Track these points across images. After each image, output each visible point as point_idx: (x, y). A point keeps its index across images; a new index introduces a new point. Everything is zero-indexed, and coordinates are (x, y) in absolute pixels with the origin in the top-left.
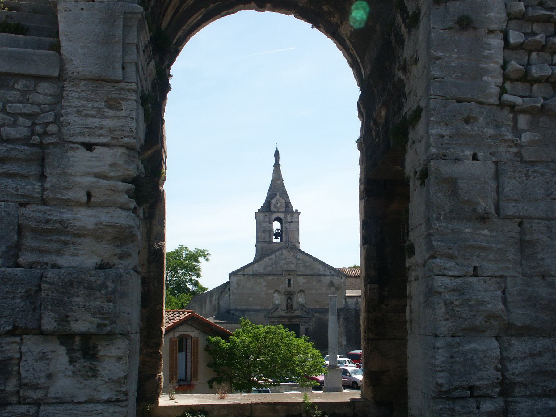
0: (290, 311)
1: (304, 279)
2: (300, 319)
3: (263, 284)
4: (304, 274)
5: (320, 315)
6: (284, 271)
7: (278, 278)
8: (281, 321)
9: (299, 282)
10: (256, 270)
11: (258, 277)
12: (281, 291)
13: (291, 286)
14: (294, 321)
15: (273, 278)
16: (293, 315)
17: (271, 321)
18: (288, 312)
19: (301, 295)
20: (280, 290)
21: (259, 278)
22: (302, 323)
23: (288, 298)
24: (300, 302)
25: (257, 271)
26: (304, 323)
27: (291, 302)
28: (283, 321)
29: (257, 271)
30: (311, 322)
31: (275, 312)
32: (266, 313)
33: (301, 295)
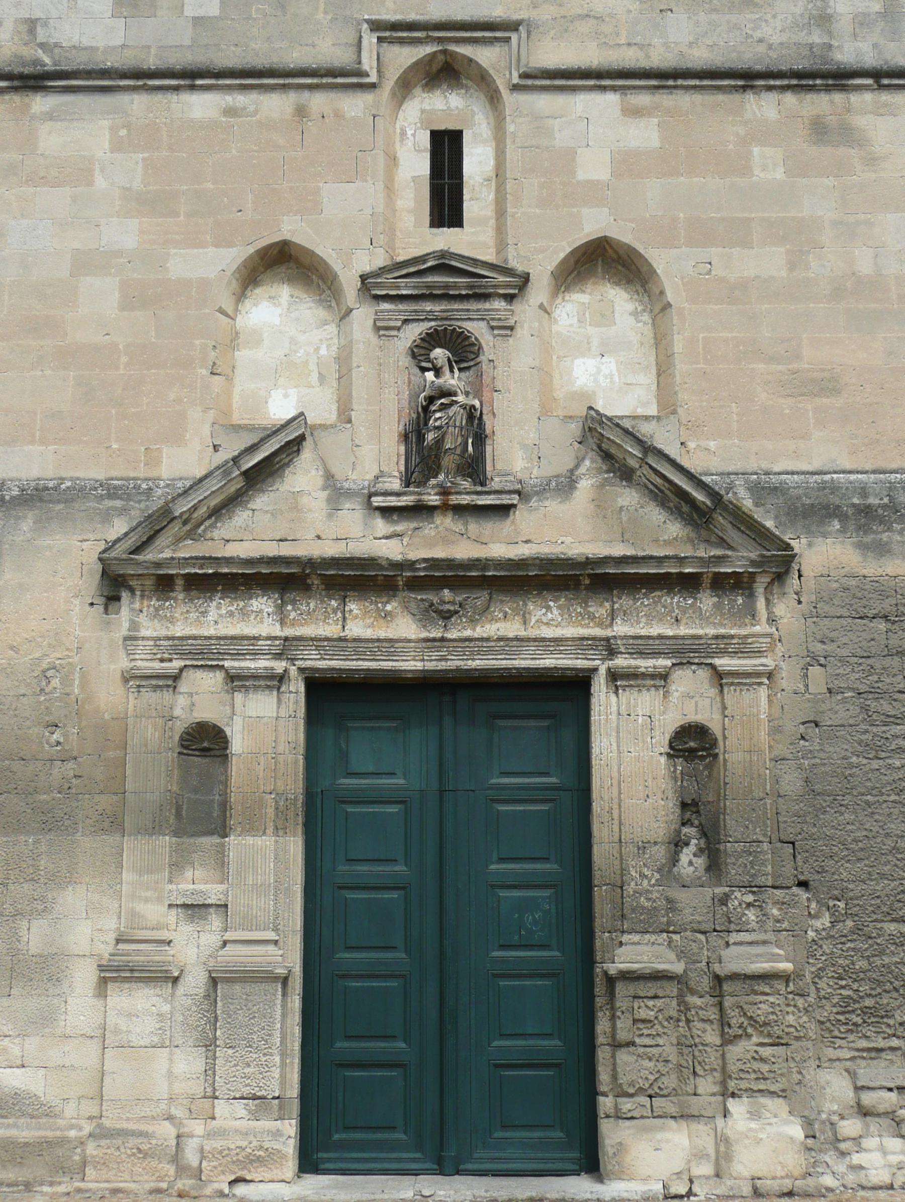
0: (445, 492)
1: (635, 113)
2: (601, 610)
3: (100, 182)
4: (630, 58)
5: (881, 550)
6: (376, 26)
7: (301, 112)
8: (330, 630)
9: (569, 156)
10: (32, 25)
11: (40, 103)
12: (336, 265)
13: (470, 208)
14: (511, 628)
15: (230, 112)
16: (499, 550)
17: (179, 630)
18: (420, 510)
19: (605, 317)
20: (325, 250)
21: (50, 116)
22: (621, 662)
23: (432, 340)
24: (582, 395)
25: (41, 35)
26: (645, 664)
27: (478, 394)
28: (357, 629)
29: (41, 35)
30: (743, 649)
31: (240, 517)
32: (119, 527)
33: (605, 317)
